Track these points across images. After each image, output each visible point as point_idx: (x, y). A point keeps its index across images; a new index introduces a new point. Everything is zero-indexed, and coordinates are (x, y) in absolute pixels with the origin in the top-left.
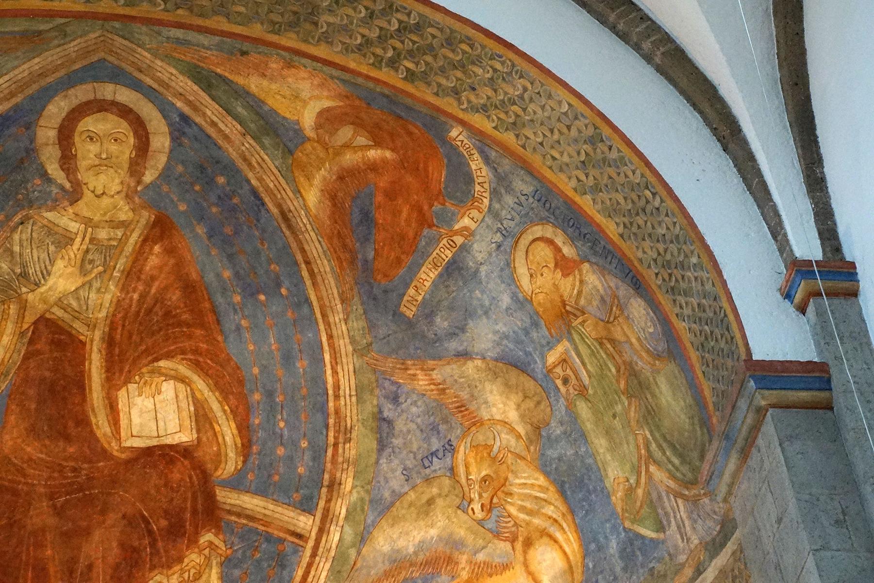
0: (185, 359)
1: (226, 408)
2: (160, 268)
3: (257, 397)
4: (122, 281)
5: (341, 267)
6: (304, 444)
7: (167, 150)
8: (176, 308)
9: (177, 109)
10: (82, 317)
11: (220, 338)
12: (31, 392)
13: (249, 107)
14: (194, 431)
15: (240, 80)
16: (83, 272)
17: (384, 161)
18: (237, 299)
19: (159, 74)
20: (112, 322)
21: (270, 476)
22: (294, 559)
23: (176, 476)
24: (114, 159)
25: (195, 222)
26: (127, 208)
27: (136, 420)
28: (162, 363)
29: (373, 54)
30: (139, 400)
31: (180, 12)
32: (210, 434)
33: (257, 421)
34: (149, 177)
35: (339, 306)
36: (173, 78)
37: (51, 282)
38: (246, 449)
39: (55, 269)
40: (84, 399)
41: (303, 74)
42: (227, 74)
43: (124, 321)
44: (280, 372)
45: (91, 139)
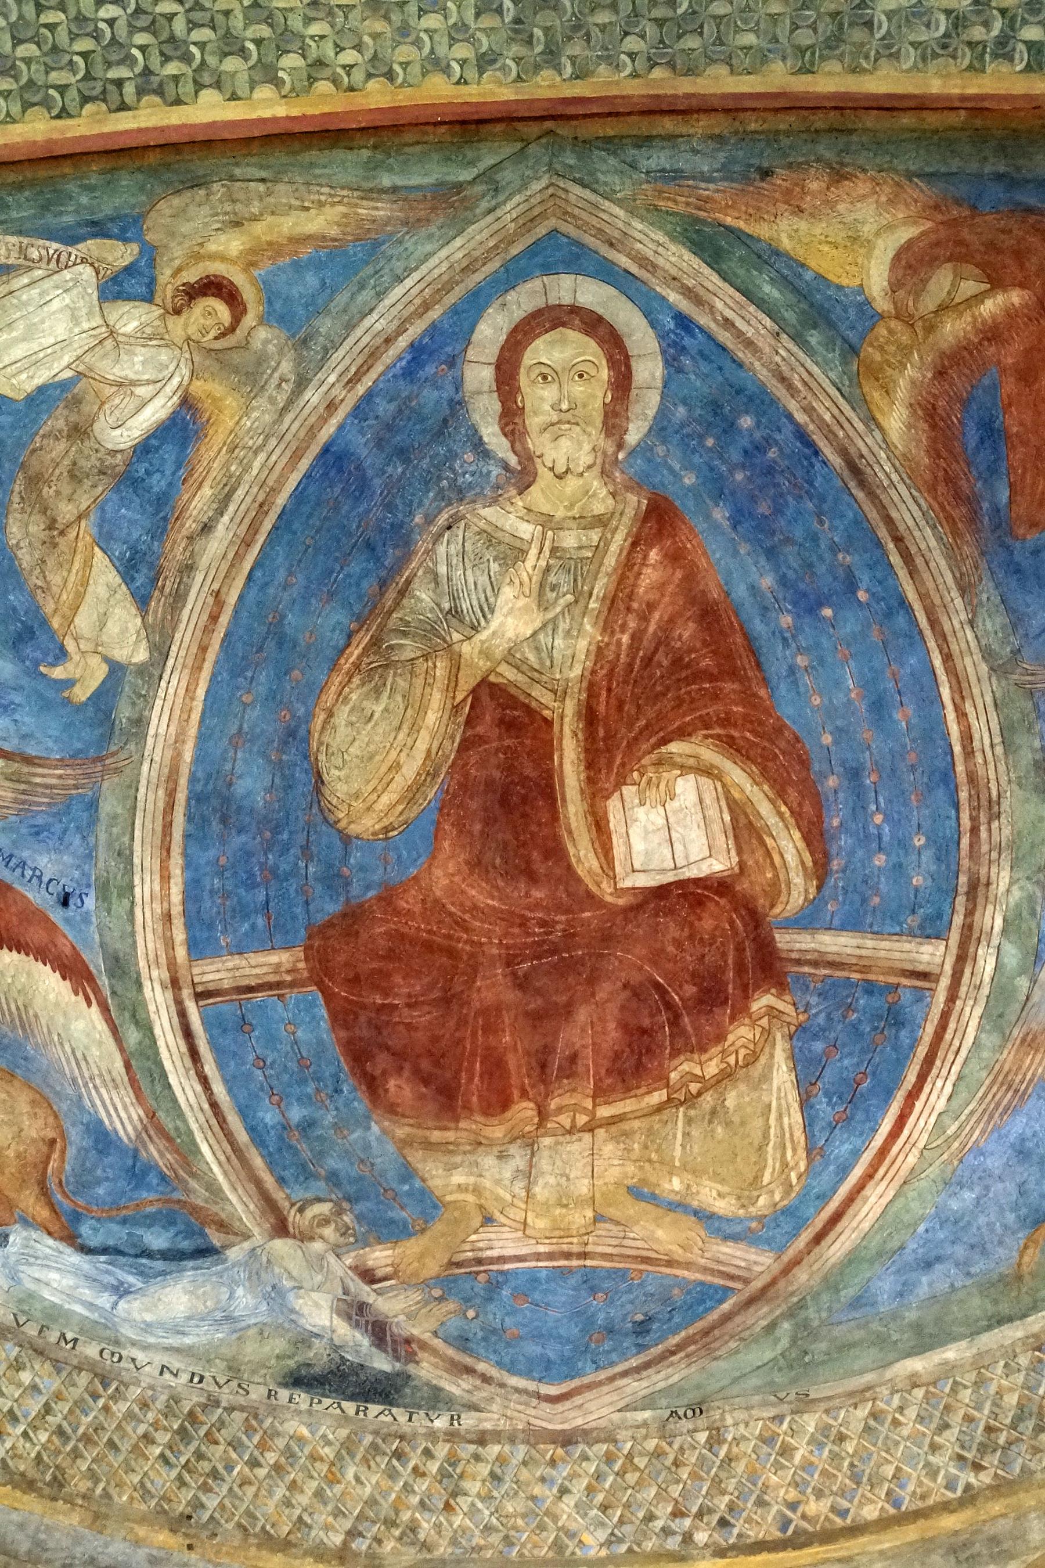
0: (711, 736)
1: (784, 809)
2: (661, 587)
3: (832, 782)
4: (603, 617)
5: (956, 533)
6: (919, 841)
7: (659, 384)
8: (690, 651)
9: (670, 307)
10: (544, 678)
11: (762, 692)
12: (474, 805)
13: (784, 282)
14: (733, 853)
15: (762, 230)
16: (543, 605)
17: (1011, 314)
18: (786, 620)
19: (639, 246)
20: (591, 685)
21: (864, 901)
22: (917, 1010)
23: (707, 924)
24: (580, 409)
25: (710, 503)
26: (604, 492)
27: (638, 845)
28: (674, 747)
29: (970, 44)
30: (641, 813)
31: (657, 73)
32: (759, 854)
33: (836, 822)
34: (634, 435)
35: (959, 602)
36: (660, 249)
37: (494, 624)
38: (820, 871)
39: (501, 599)
40: (555, 818)
41: (863, 187)
42: (741, 224)
43: (610, 681)
44: (866, 734)
45: (545, 378)
